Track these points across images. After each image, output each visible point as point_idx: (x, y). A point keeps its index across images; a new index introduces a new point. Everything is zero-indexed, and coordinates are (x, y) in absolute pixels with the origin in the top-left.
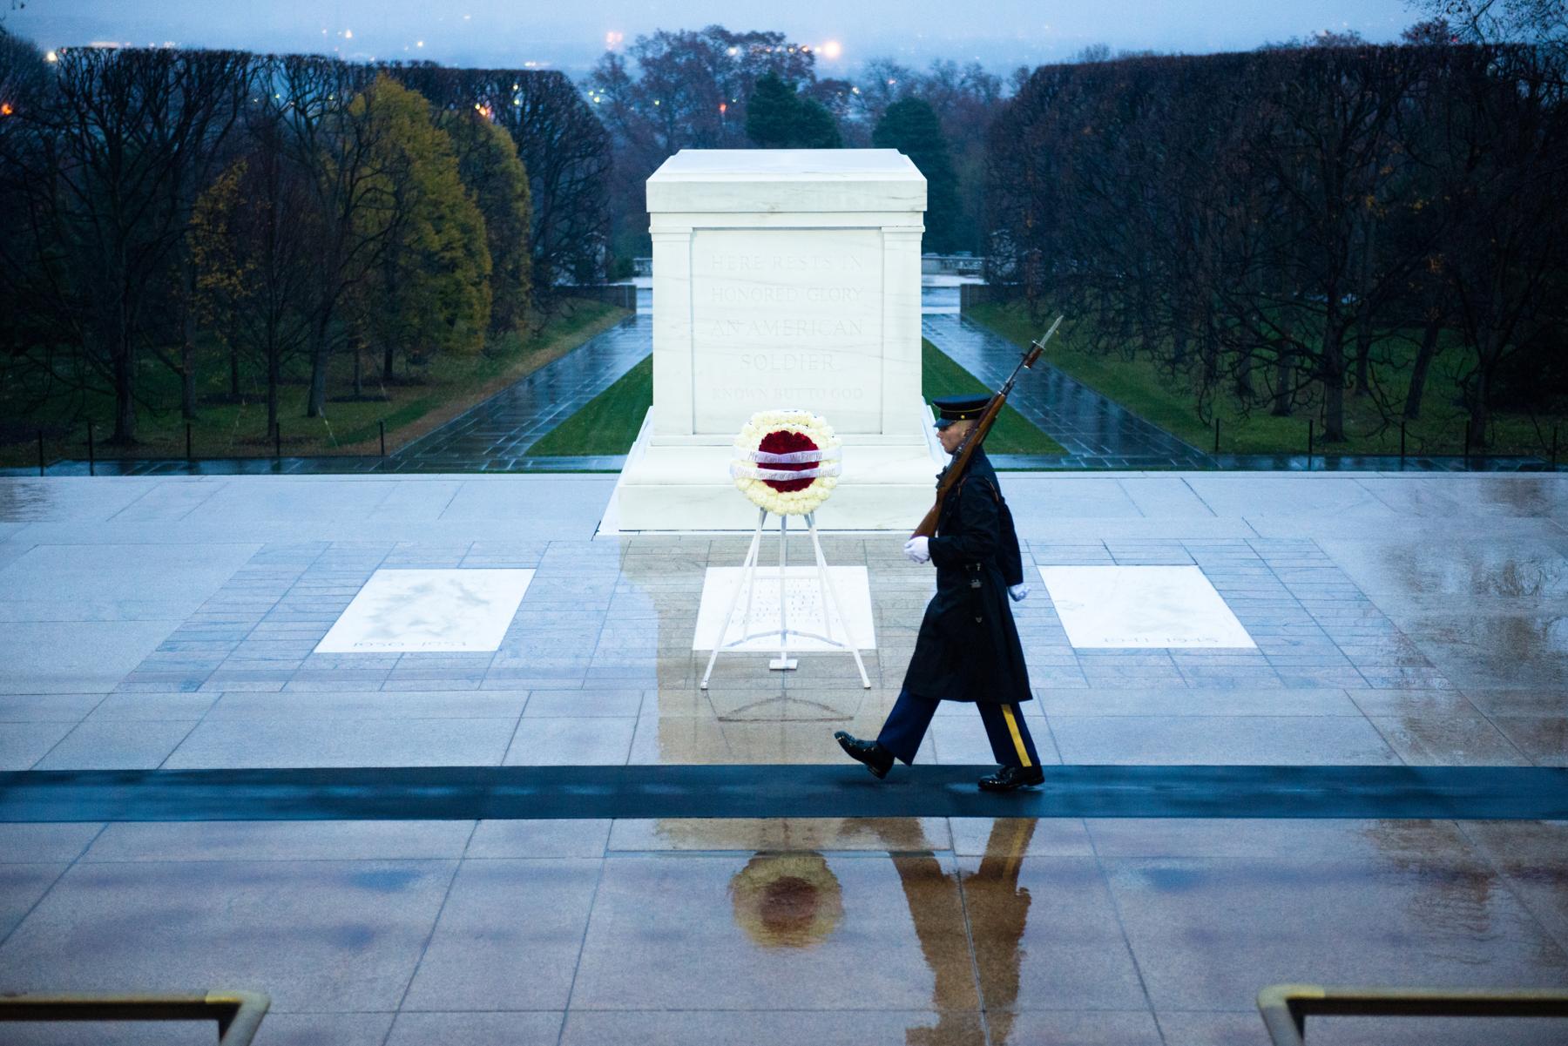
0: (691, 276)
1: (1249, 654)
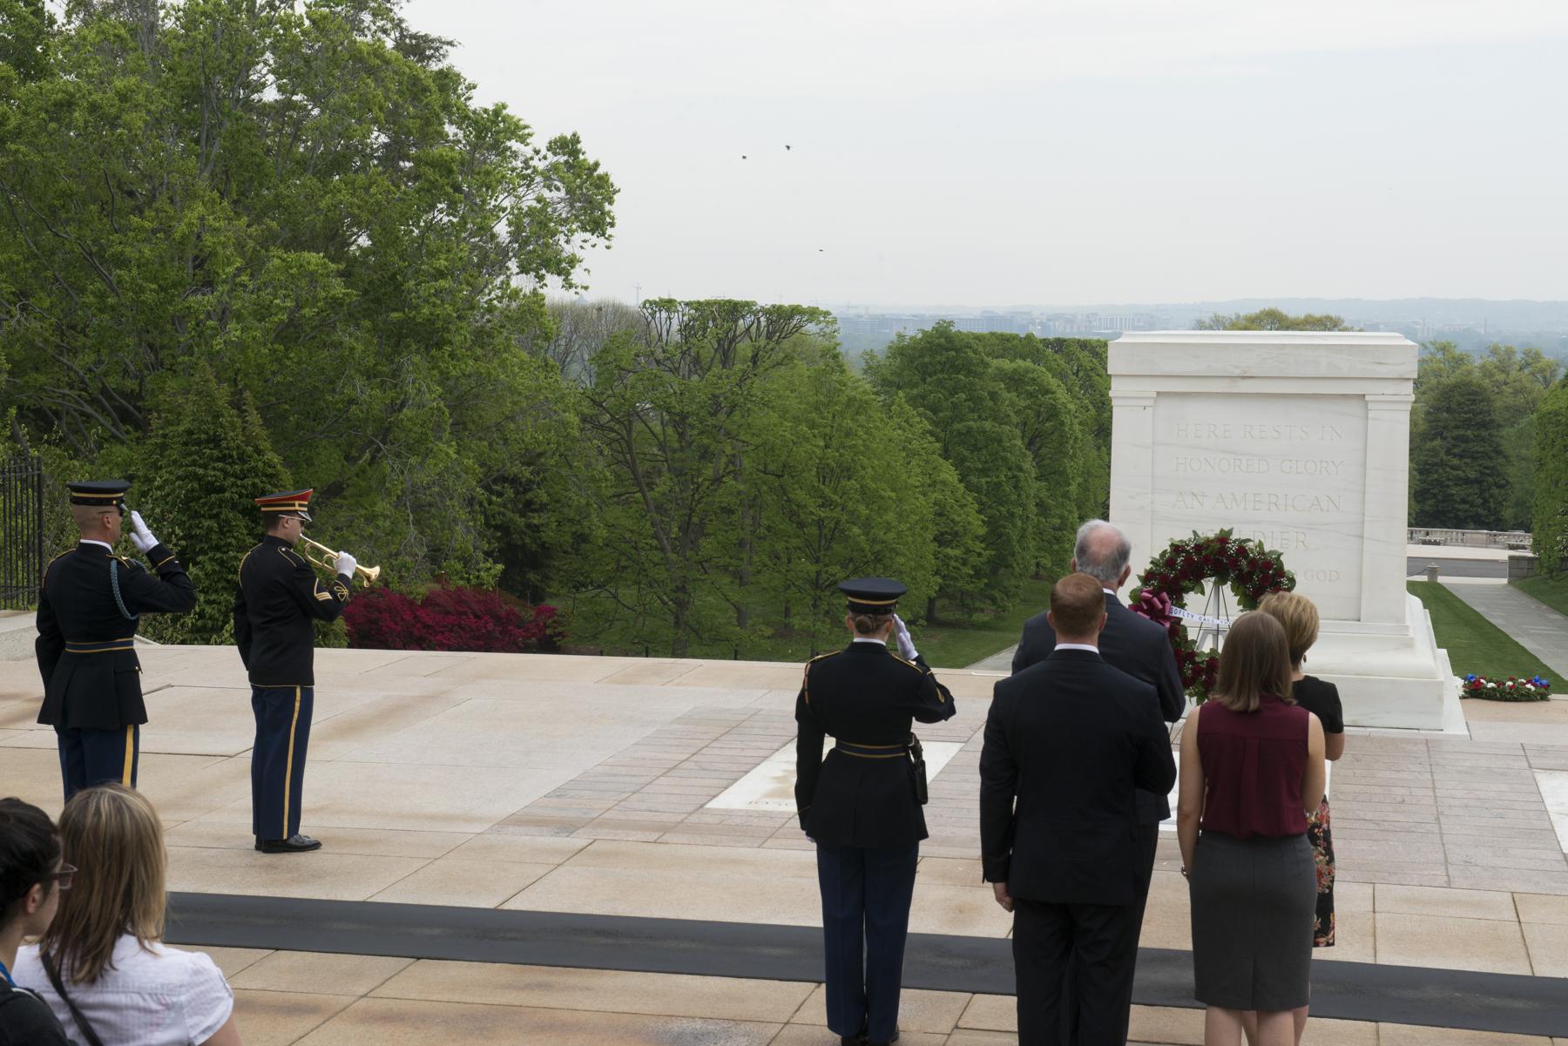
0: (1153, 443)
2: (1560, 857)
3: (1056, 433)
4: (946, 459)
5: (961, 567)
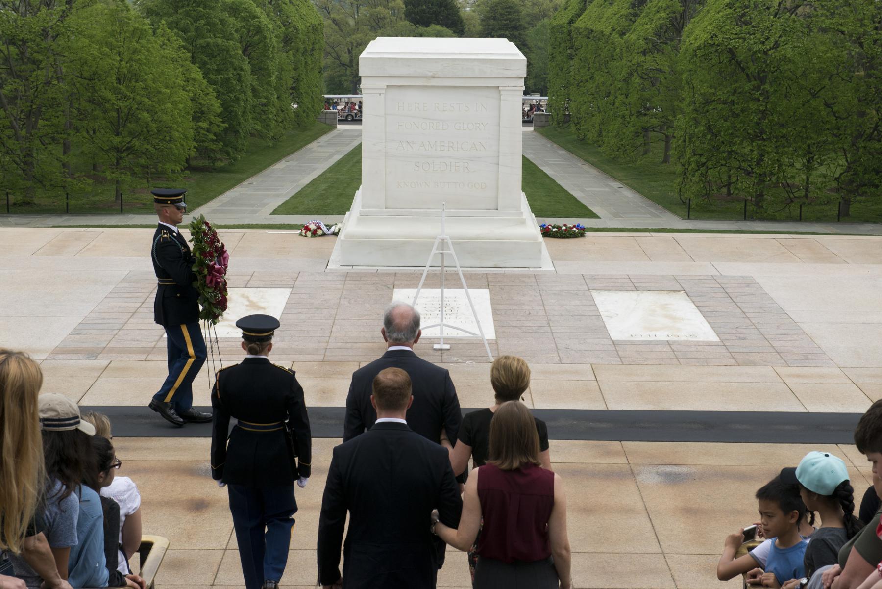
1: (716, 345)
2: (611, 343)
3: (261, 44)
4: (193, 62)
5: (208, 134)
